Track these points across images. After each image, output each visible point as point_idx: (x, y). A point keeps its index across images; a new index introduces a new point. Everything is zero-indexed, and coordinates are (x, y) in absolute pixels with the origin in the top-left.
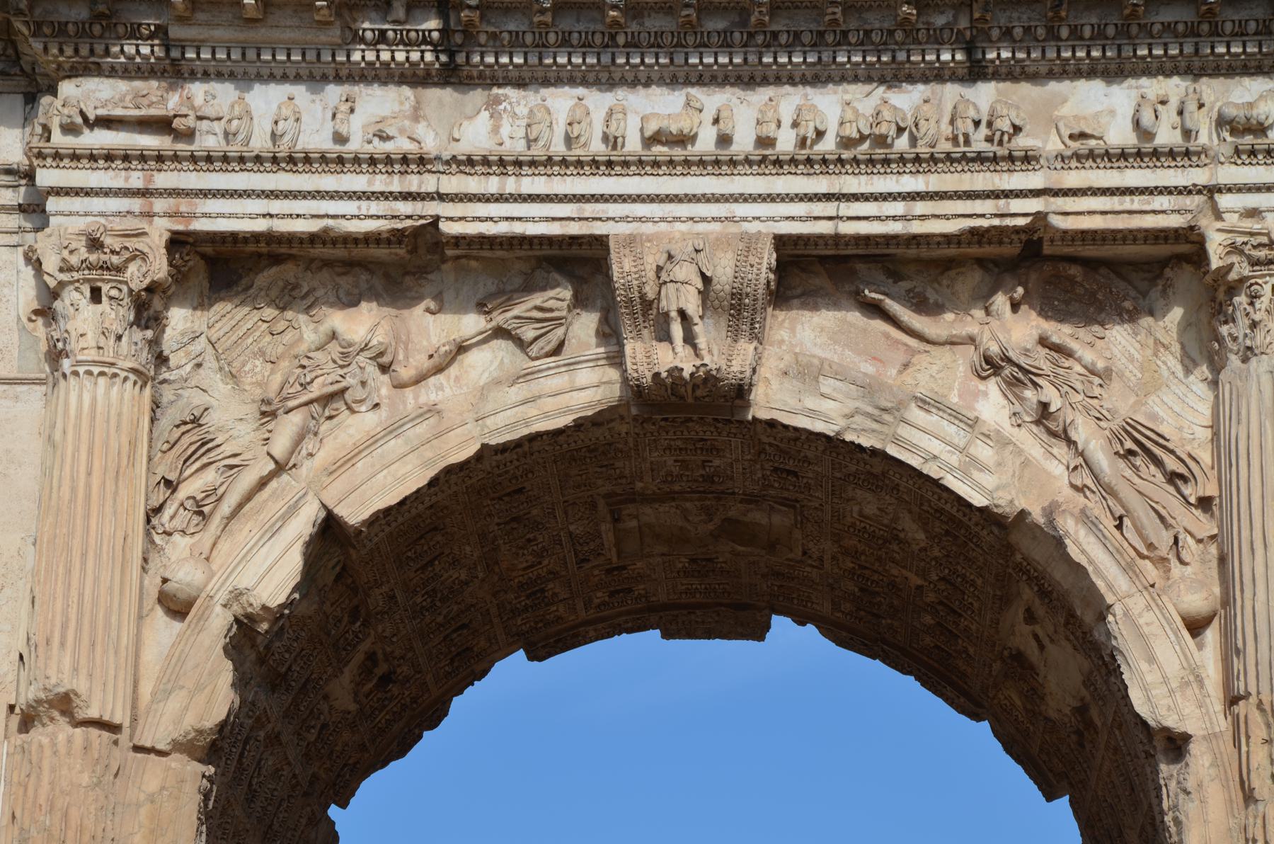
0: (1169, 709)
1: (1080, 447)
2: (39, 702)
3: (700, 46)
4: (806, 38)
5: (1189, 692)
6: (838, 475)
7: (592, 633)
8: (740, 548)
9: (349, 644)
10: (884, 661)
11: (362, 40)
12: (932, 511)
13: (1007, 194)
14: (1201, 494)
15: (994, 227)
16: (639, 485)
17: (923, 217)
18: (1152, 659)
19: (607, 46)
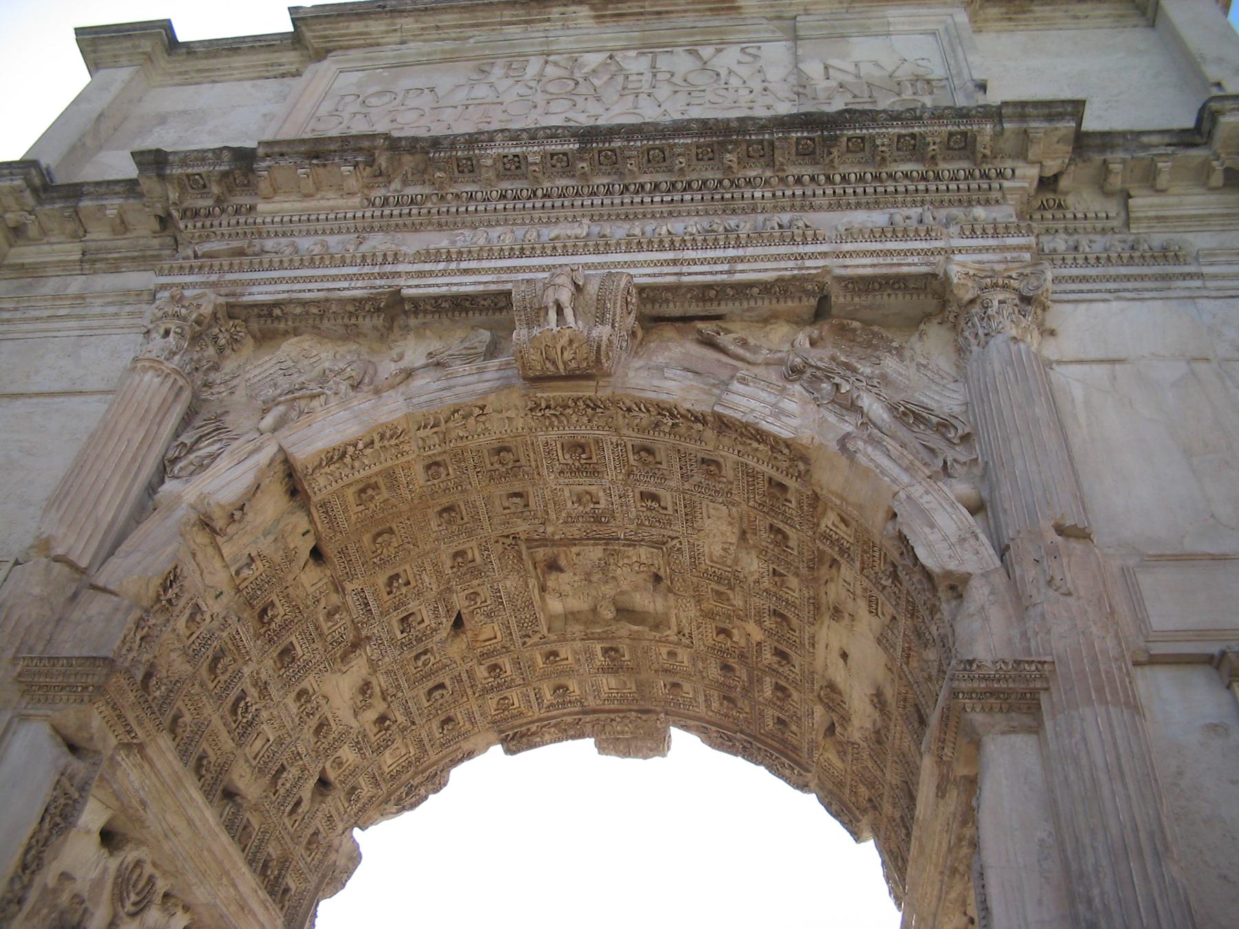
0: (950, 557)
1: (865, 410)
2: (32, 547)
3: (591, 194)
4: (663, 186)
5: (966, 545)
6: (687, 486)
7: (547, 737)
8: (635, 628)
9: (335, 641)
10: (743, 757)
11: (373, 205)
12: (756, 505)
13: (802, 257)
14: (960, 432)
15: (794, 277)
16: (550, 529)
17: (742, 271)
18: (932, 526)
19: (530, 198)
